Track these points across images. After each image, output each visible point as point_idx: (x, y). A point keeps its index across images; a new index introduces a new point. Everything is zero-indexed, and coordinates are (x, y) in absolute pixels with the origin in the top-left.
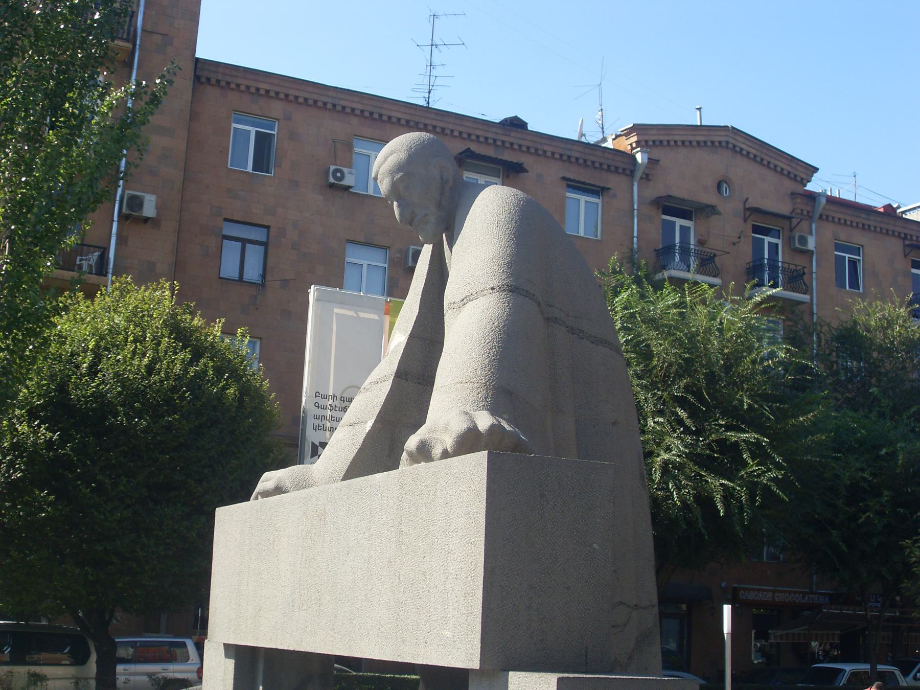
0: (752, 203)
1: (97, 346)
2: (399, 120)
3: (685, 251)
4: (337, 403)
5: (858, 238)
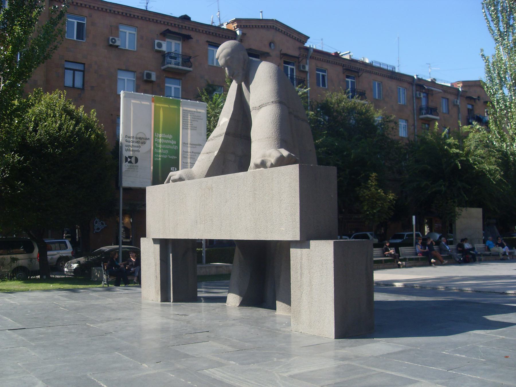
0: (284, 52)
1: (35, 119)
2: (138, 16)
4: (135, 140)
5: (325, 66)
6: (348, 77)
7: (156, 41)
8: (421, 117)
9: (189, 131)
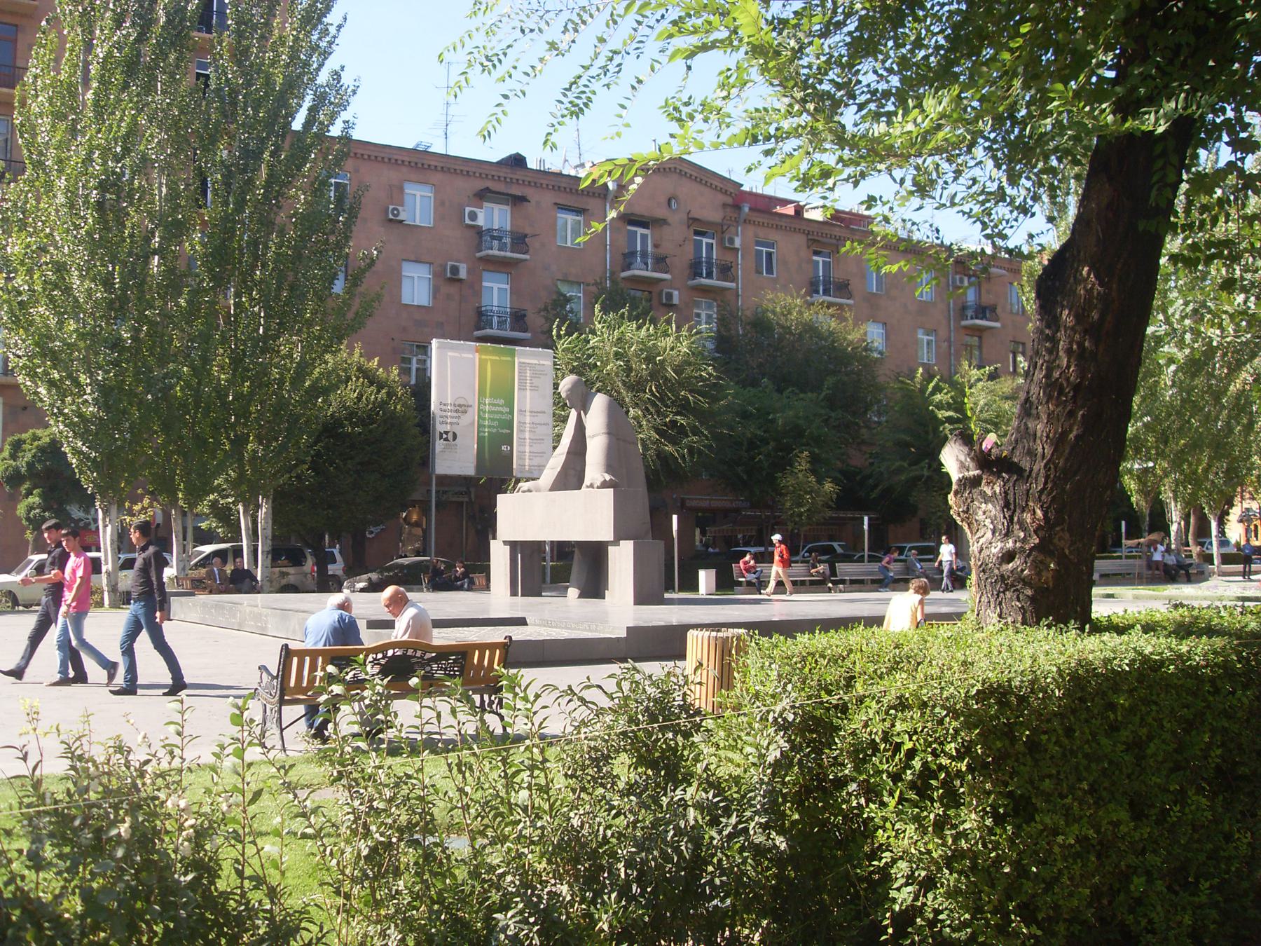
0: (694, 214)
3: (644, 254)
5: (774, 236)
6: (817, 253)
7: (468, 209)
8: (964, 323)
9: (528, 392)
